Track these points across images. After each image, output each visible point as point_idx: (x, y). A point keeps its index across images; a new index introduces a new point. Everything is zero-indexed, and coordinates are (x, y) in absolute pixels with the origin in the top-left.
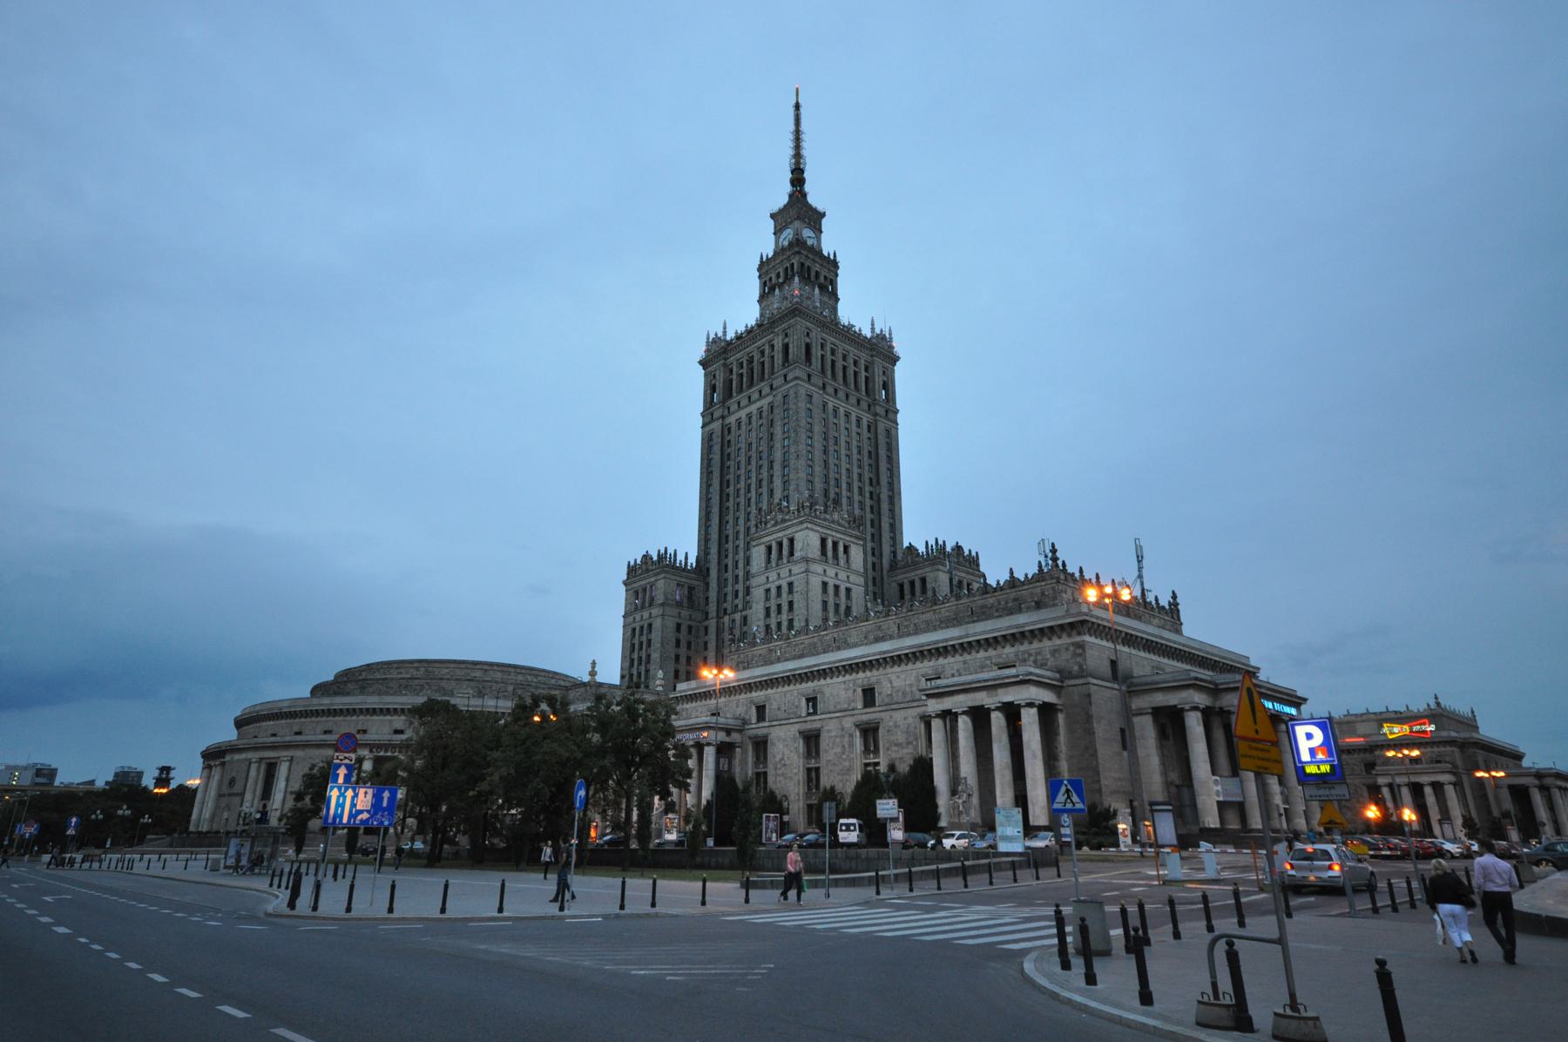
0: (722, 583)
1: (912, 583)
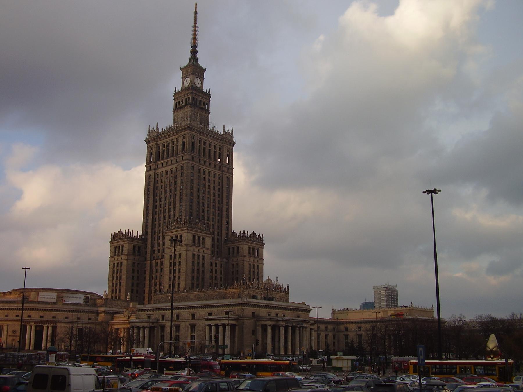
0: (153, 245)
1: (234, 248)
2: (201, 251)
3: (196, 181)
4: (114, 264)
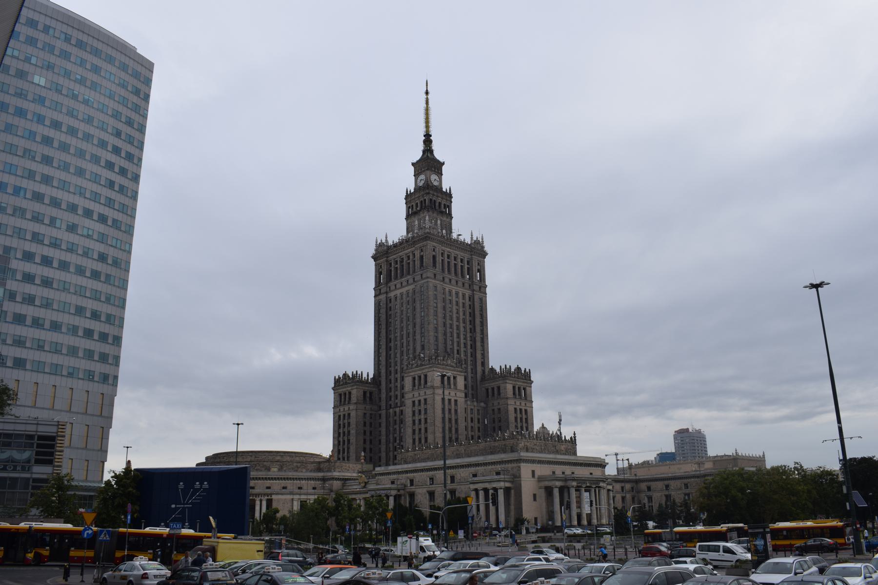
0: (389, 390)
1: (493, 389)
2: (453, 393)
4: (340, 416)
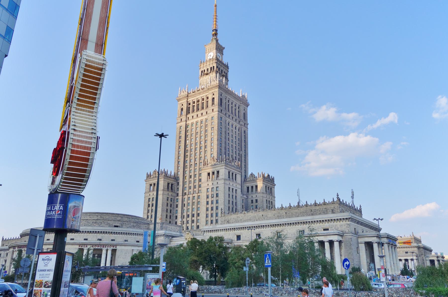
1: (252, 187)
3: (223, 130)
